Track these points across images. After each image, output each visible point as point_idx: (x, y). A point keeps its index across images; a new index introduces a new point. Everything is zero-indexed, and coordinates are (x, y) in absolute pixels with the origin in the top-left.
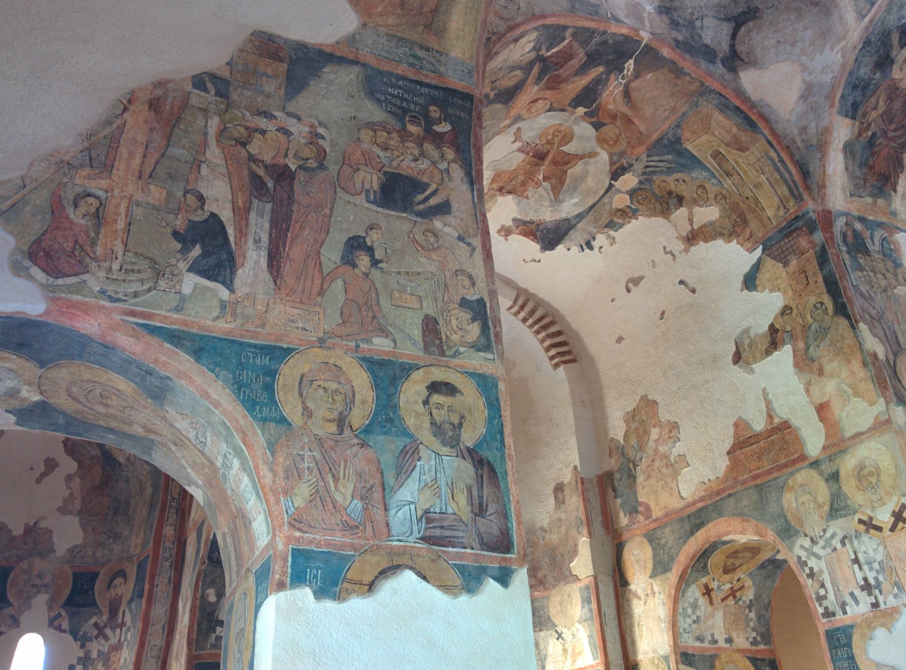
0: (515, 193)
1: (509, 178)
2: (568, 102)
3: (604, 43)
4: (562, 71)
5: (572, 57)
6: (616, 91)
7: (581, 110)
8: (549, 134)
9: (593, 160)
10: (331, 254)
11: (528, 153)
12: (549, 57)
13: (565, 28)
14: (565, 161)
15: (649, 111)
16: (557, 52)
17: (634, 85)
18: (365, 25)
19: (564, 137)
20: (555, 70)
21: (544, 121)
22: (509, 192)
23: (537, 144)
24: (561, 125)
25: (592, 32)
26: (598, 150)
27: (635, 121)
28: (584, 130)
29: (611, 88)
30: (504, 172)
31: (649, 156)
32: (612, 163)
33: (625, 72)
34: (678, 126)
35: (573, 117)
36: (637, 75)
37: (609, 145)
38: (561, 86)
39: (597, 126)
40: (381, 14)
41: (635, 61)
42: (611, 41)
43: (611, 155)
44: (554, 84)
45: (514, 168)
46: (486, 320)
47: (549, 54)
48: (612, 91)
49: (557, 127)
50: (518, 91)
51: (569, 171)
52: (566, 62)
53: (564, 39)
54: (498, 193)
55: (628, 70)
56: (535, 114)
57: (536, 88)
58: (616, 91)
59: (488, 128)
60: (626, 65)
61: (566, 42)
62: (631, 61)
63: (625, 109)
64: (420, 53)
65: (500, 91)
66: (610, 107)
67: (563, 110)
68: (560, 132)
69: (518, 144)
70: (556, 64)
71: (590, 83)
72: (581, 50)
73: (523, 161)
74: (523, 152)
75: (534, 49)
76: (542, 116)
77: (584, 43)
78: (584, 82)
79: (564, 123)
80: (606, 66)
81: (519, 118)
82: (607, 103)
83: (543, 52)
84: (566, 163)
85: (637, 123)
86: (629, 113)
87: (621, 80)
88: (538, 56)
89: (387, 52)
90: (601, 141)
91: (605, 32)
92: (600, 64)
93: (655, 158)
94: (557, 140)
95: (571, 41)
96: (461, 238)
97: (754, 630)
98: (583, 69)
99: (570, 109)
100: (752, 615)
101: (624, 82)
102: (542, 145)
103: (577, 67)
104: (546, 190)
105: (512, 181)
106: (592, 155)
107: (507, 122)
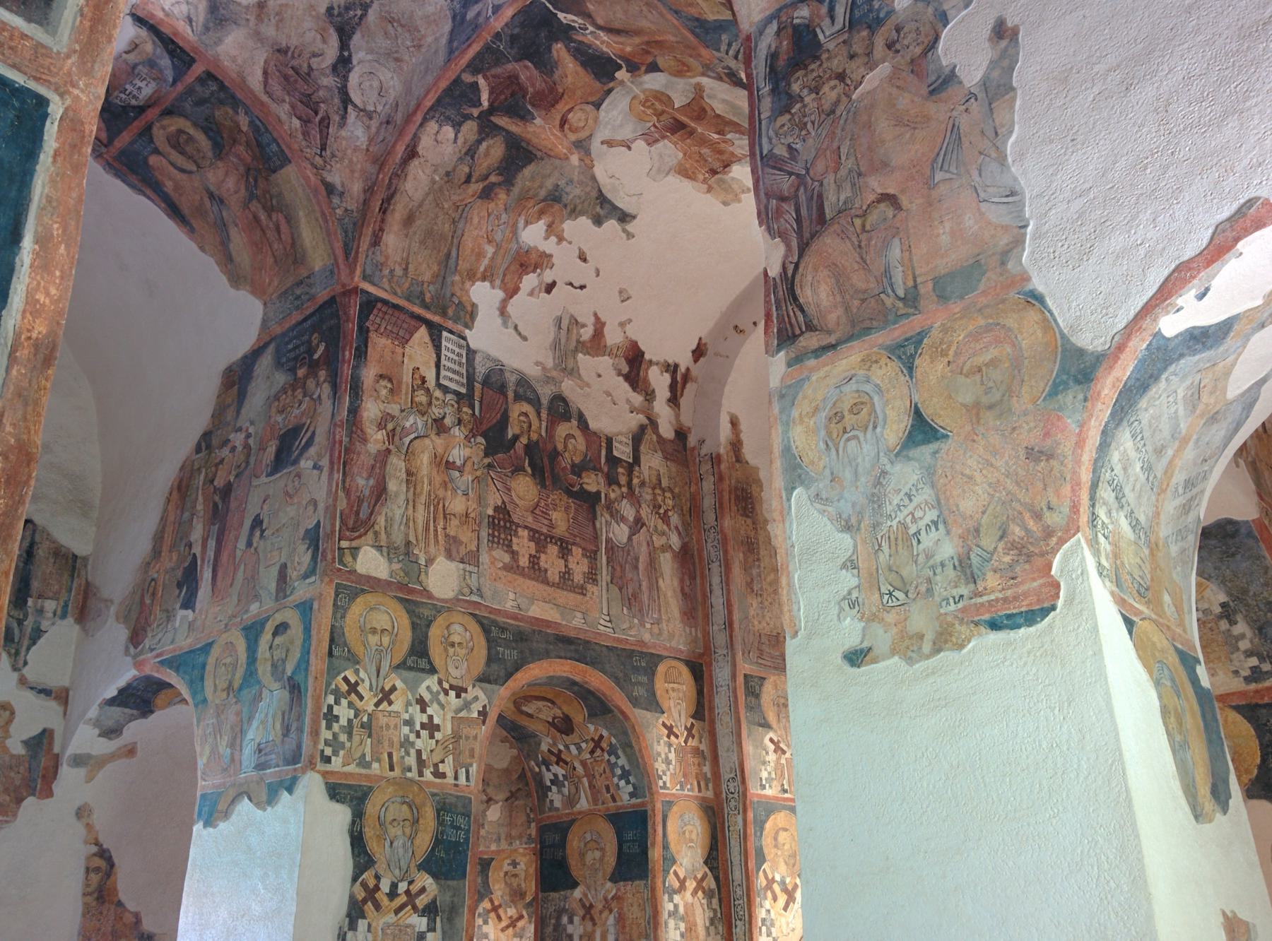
0: (732, 162)
1: (697, 161)
2: (598, 84)
3: (514, 39)
4: (531, 90)
5: (513, 78)
6: (606, 38)
7: (622, 75)
8: (643, 112)
9: (707, 91)
10: (242, 544)
11: (664, 137)
12: (491, 105)
13: (457, 81)
14: (698, 108)
15: (644, 23)
16: (491, 93)
17: (600, 22)
18: (265, 304)
19: (656, 98)
20: (524, 97)
21: (615, 113)
22: (727, 165)
23: (654, 125)
24: (634, 98)
25: (487, 48)
26: (694, 81)
27: (658, 38)
28: (654, 81)
29: (598, 43)
30: (680, 164)
31: (718, 50)
32: (720, 79)
33: (577, 25)
34: (676, 12)
35: (629, 84)
36: (588, 16)
37: (688, 71)
38: (561, 90)
39: (654, 68)
40: (270, 284)
41: (563, 12)
42: (516, 31)
43: (703, 74)
44: (549, 99)
45: (681, 155)
46: (318, 541)
47: (486, 104)
48: (603, 42)
49: (636, 102)
50: (524, 144)
51: (717, 112)
52: (519, 84)
53: (475, 86)
54: (717, 176)
55: (574, 21)
56: (590, 121)
57: (538, 121)
58: (606, 38)
59: (562, 183)
60: (565, 22)
61: (482, 82)
62: (561, 15)
63: (637, 40)
64: (298, 292)
65: (498, 168)
66: (628, 49)
67: (609, 91)
68: (647, 100)
69: (640, 145)
70: (512, 95)
71: (576, 59)
72: (509, 66)
73: (675, 144)
74: (657, 141)
75: (457, 126)
76: (602, 113)
77: (499, 58)
78: (571, 65)
79: (632, 95)
80: (557, 41)
81: (582, 146)
82: (622, 50)
83: (476, 112)
84: (704, 110)
85: (661, 38)
86: (646, 39)
87: (588, 32)
88: (479, 117)
89: (282, 312)
90: (679, 73)
91: (498, 36)
92: (549, 49)
93: (724, 47)
94: (658, 106)
95: (485, 77)
96: (315, 467)
97: (1249, 654)
98: (545, 65)
99: (611, 85)
100: (1241, 627)
101: (591, 28)
102: (659, 121)
103: (535, 72)
104: (741, 139)
105: (706, 161)
106: (699, 89)
107: (575, 159)
